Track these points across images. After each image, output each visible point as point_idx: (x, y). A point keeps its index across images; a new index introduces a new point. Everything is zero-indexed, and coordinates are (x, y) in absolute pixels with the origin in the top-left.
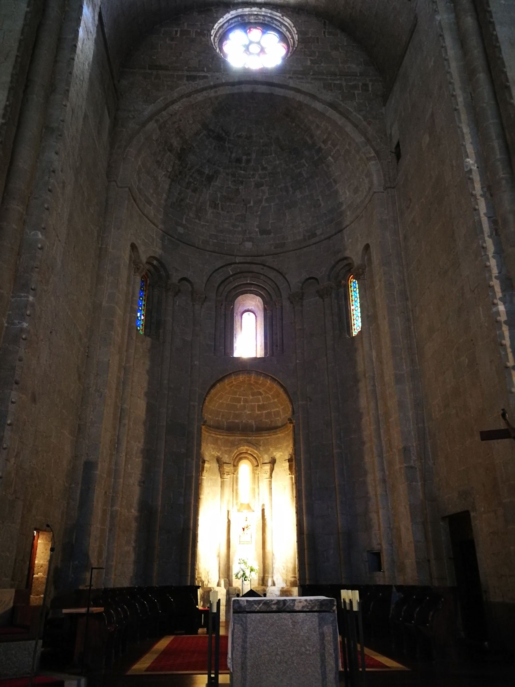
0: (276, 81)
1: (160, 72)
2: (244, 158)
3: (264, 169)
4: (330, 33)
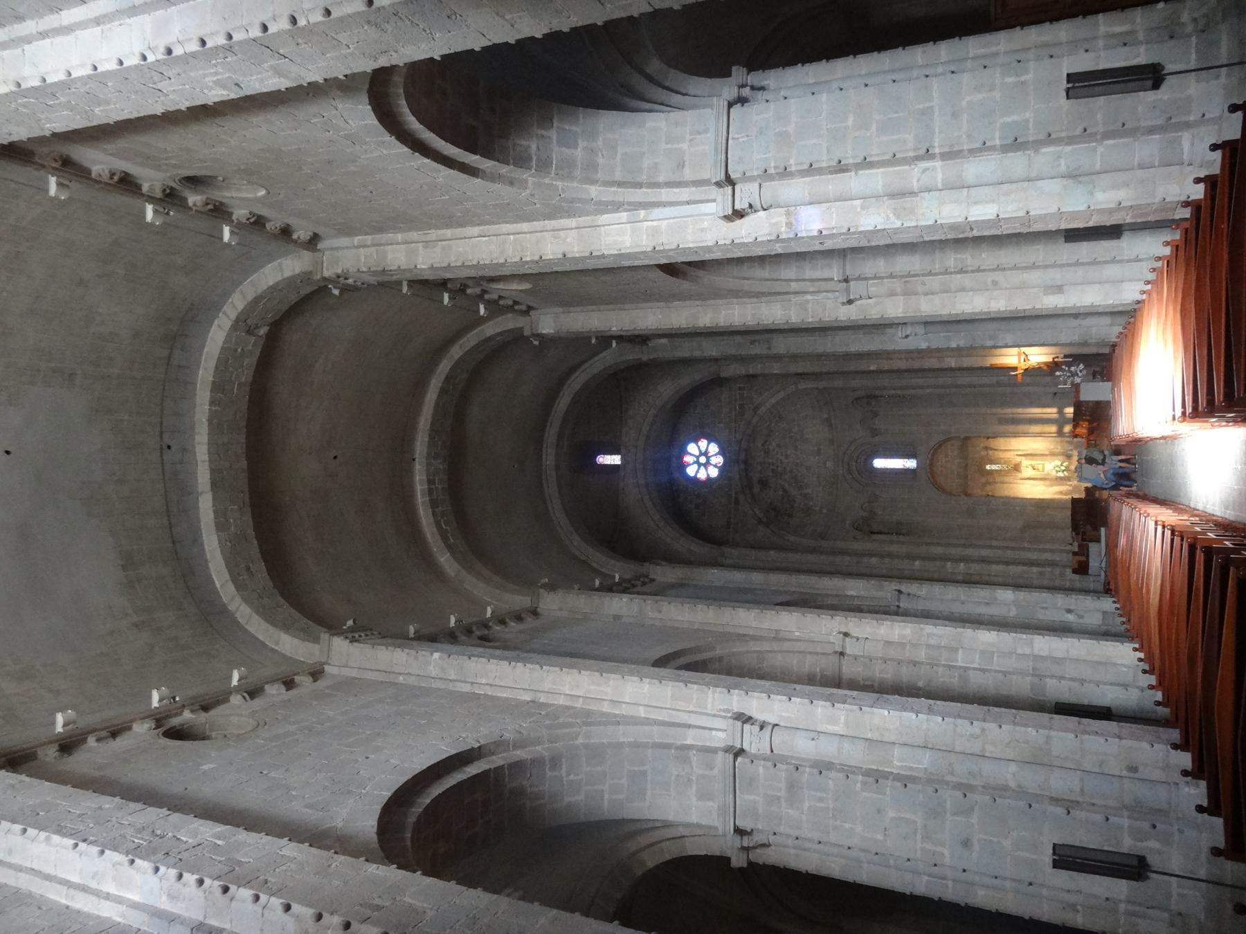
1: (732, 521)
3: (777, 454)
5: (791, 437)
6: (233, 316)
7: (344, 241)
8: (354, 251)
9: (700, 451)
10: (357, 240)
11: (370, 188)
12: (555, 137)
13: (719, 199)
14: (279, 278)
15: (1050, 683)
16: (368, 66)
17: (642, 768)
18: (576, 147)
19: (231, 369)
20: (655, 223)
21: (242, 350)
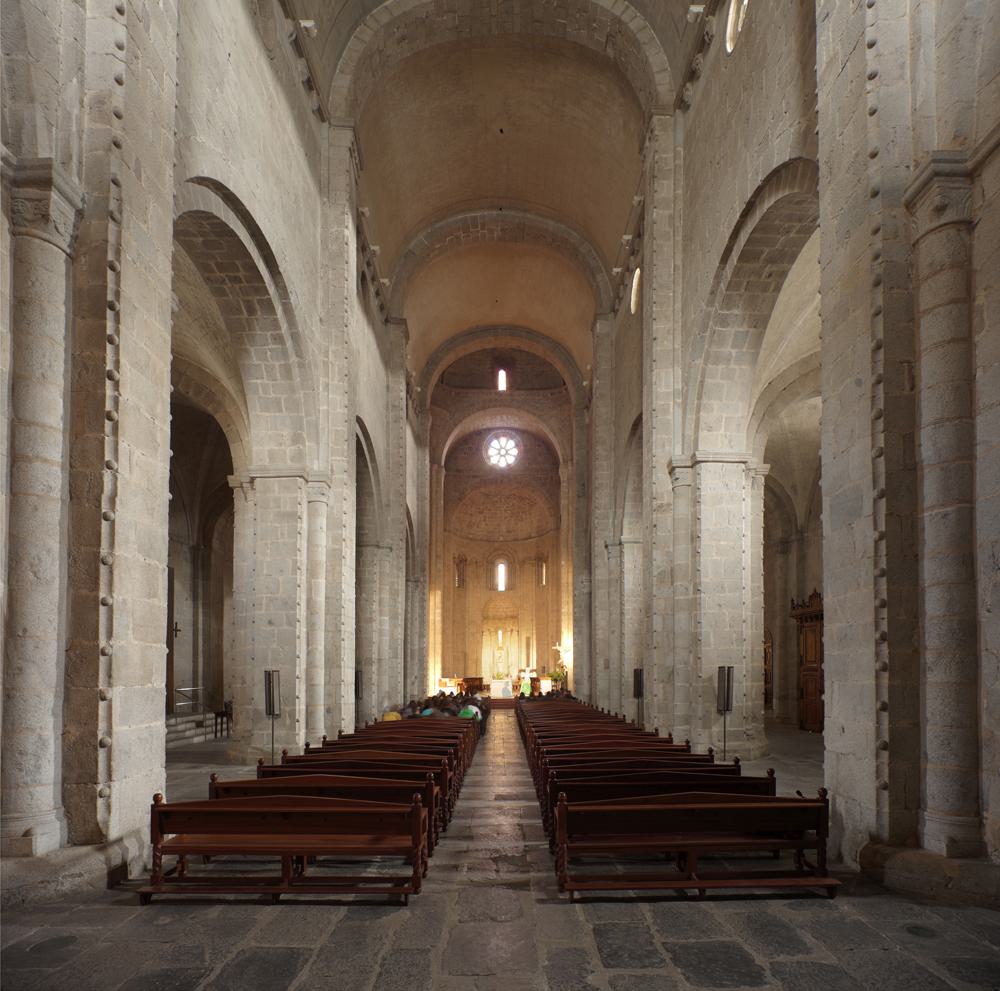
4: (539, 446)
6: (625, 18)
7: (681, 136)
8: (672, 147)
10: (680, 149)
11: (722, 163)
12: (741, 329)
13: (683, 457)
14: (655, 69)
15: (374, 668)
16: (822, 156)
17: (284, 409)
18: (732, 347)
19: (578, 15)
20: (671, 410)
21: (595, 28)
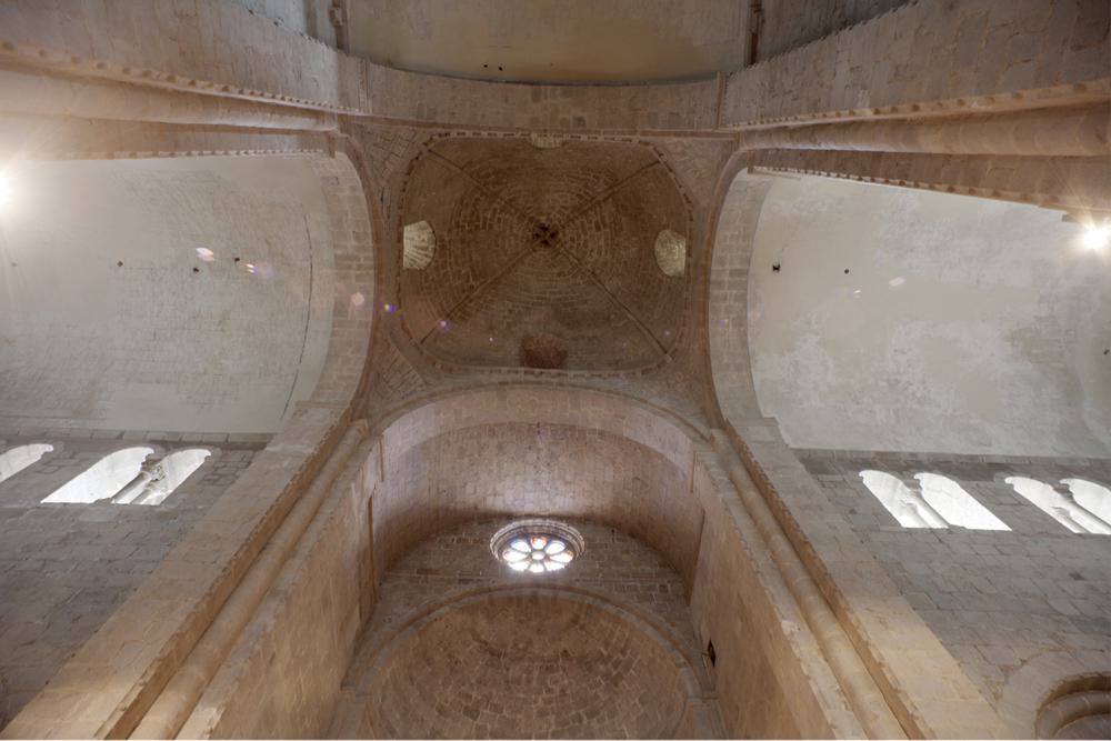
0: (559, 583)
1: (429, 576)
2: (524, 676)
3: (549, 691)
5: (580, 720)
9: (553, 555)
